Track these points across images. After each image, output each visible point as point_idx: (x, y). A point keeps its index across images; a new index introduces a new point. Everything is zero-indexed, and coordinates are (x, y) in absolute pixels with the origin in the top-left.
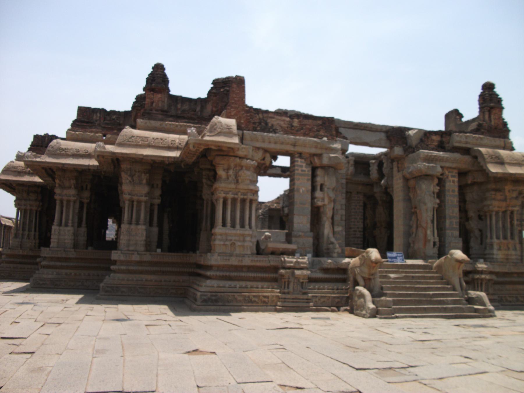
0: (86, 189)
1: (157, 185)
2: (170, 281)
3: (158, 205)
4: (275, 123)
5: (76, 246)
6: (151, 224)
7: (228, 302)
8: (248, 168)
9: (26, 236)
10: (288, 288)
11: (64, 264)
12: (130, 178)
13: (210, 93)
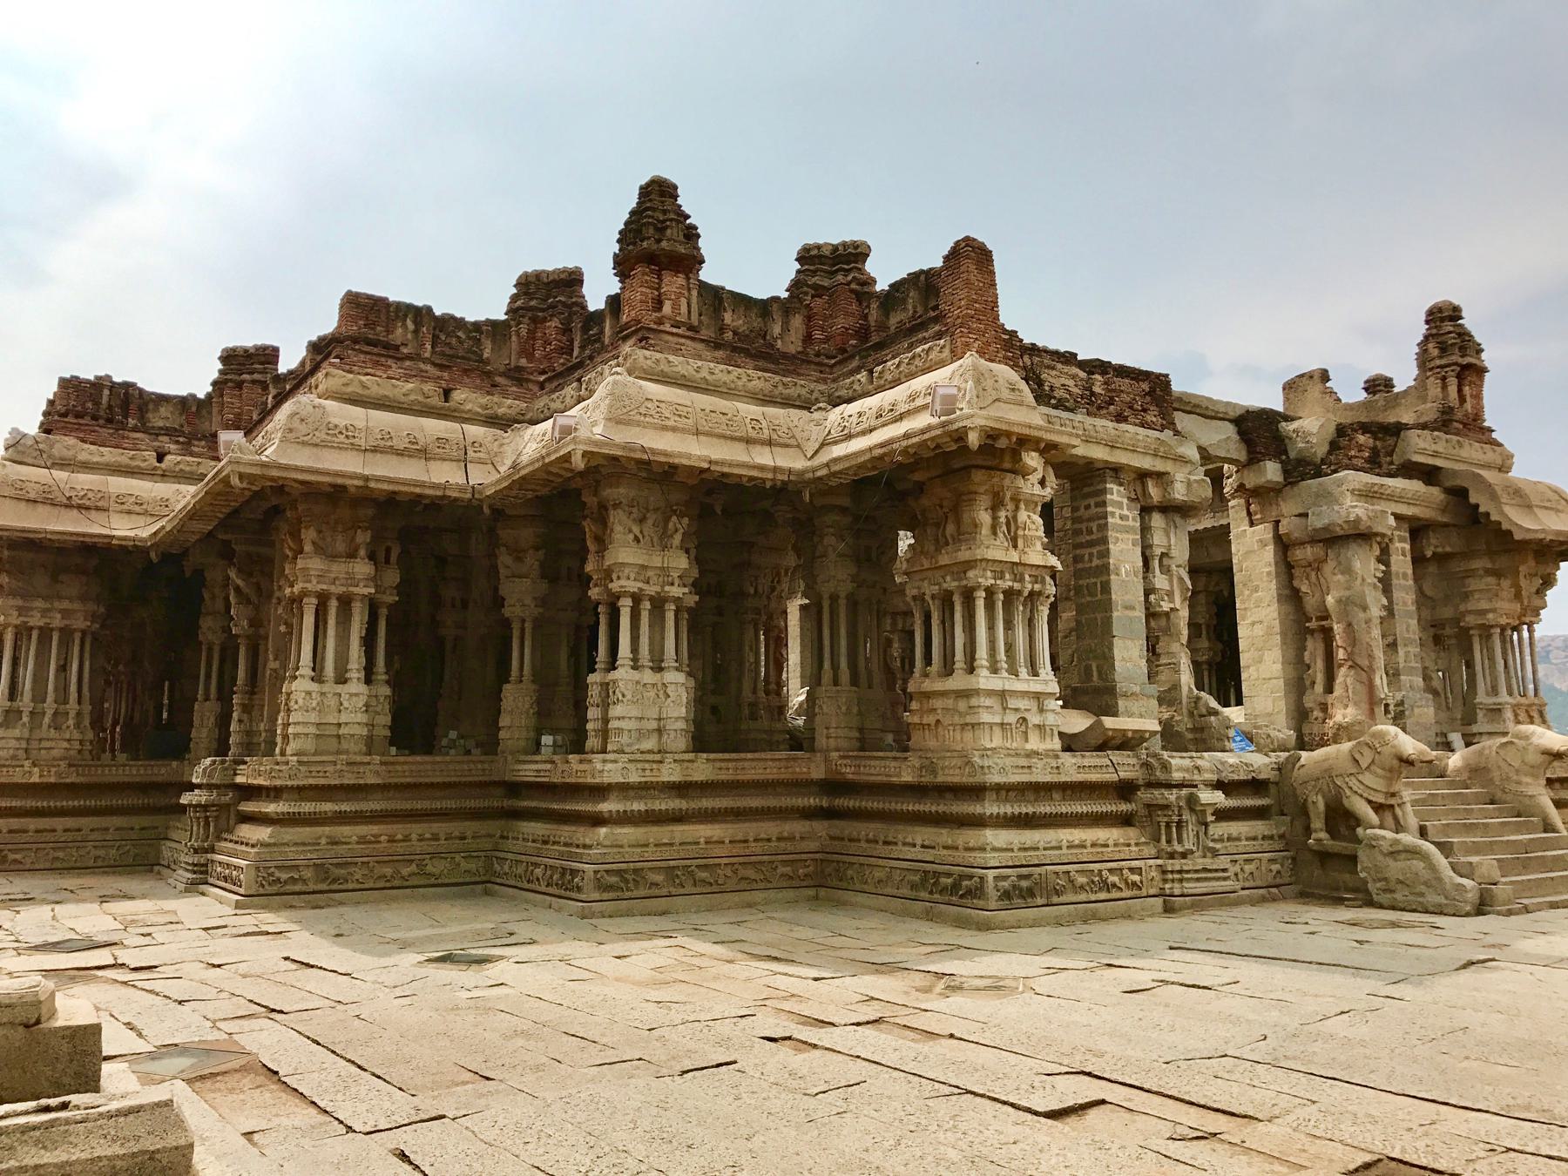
0: (387, 561)
2: (769, 840)
4: (1057, 383)
7: (1058, 893)
9: (47, 720)
10: (1180, 841)
13: (795, 286)
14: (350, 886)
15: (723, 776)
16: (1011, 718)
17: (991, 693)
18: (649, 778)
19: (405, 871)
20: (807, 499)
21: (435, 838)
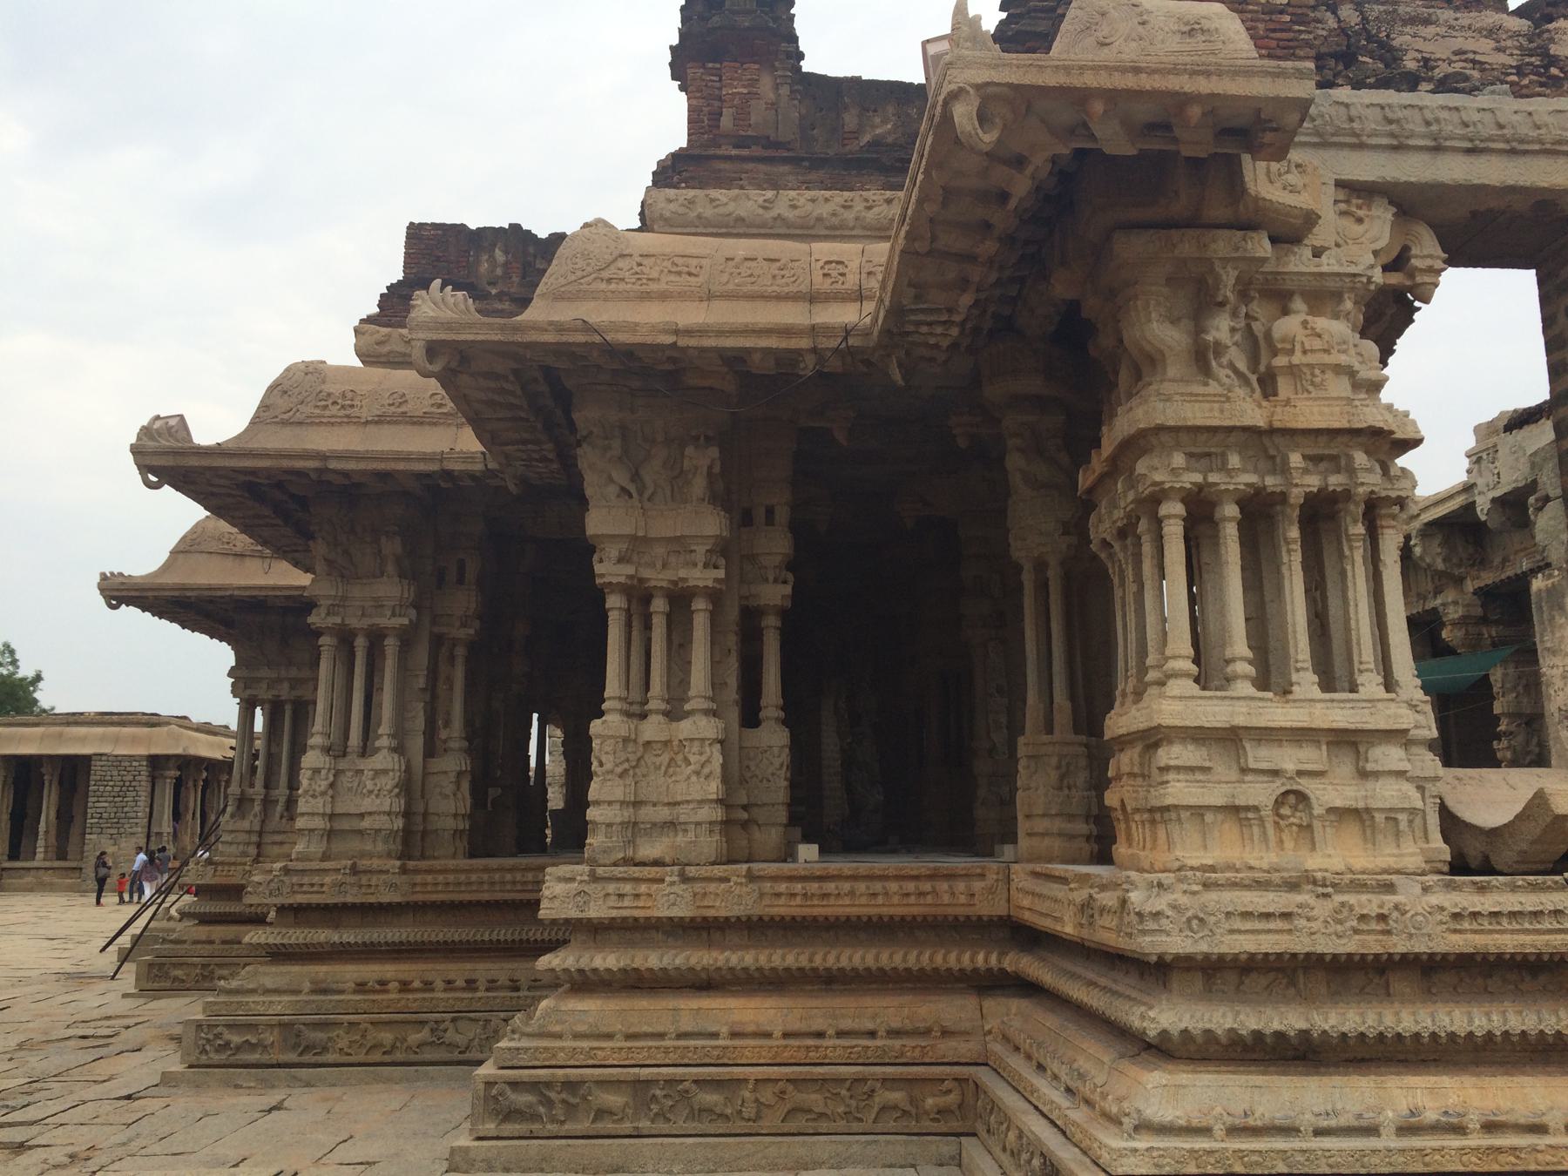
1: (770, 512)
3: (783, 613)
5: (413, 840)
6: (750, 718)
8: (1322, 296)
9: (279, 808)
11: (349, 936)
12: (621, 477)
14: (330, 1057)
15: (781, 909)
16: (1261, 793)
17: (1199, 735)
18: (630, 910)
19: (415, 1037)
20: (897, 376)
21: (471, 984)
